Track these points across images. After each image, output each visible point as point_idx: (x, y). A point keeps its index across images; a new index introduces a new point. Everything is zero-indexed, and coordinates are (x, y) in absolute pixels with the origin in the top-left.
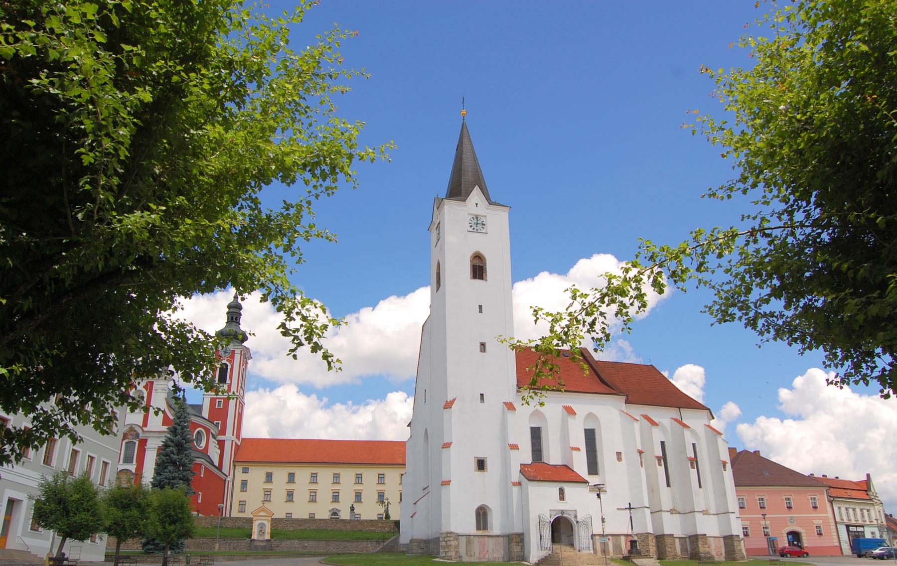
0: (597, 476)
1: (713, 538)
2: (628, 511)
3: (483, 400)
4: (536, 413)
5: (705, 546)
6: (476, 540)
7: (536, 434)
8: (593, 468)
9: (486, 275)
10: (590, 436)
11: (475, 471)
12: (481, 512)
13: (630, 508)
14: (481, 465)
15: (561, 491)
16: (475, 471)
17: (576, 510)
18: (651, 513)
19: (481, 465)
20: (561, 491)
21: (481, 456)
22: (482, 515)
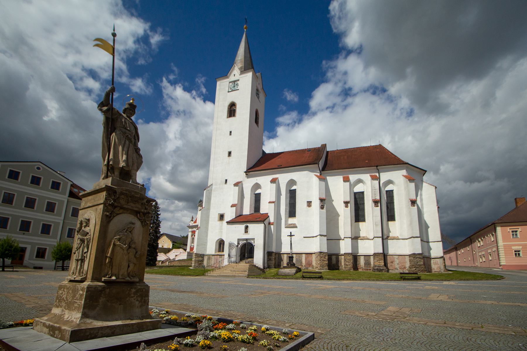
0: (295, 218)
1: (398, 256)
2: (289, 238)
5: (380, 261)
6: (213, 257)
7: (257, 198)
8: (292, 213)
10: (292, 195)
11: (218, 221)
12: (222, 243)
15: (247, 227)
16: (218, 221)
18: (327, 240)
20: (247, 227)
21: (221, 212)
22: (221, 244)
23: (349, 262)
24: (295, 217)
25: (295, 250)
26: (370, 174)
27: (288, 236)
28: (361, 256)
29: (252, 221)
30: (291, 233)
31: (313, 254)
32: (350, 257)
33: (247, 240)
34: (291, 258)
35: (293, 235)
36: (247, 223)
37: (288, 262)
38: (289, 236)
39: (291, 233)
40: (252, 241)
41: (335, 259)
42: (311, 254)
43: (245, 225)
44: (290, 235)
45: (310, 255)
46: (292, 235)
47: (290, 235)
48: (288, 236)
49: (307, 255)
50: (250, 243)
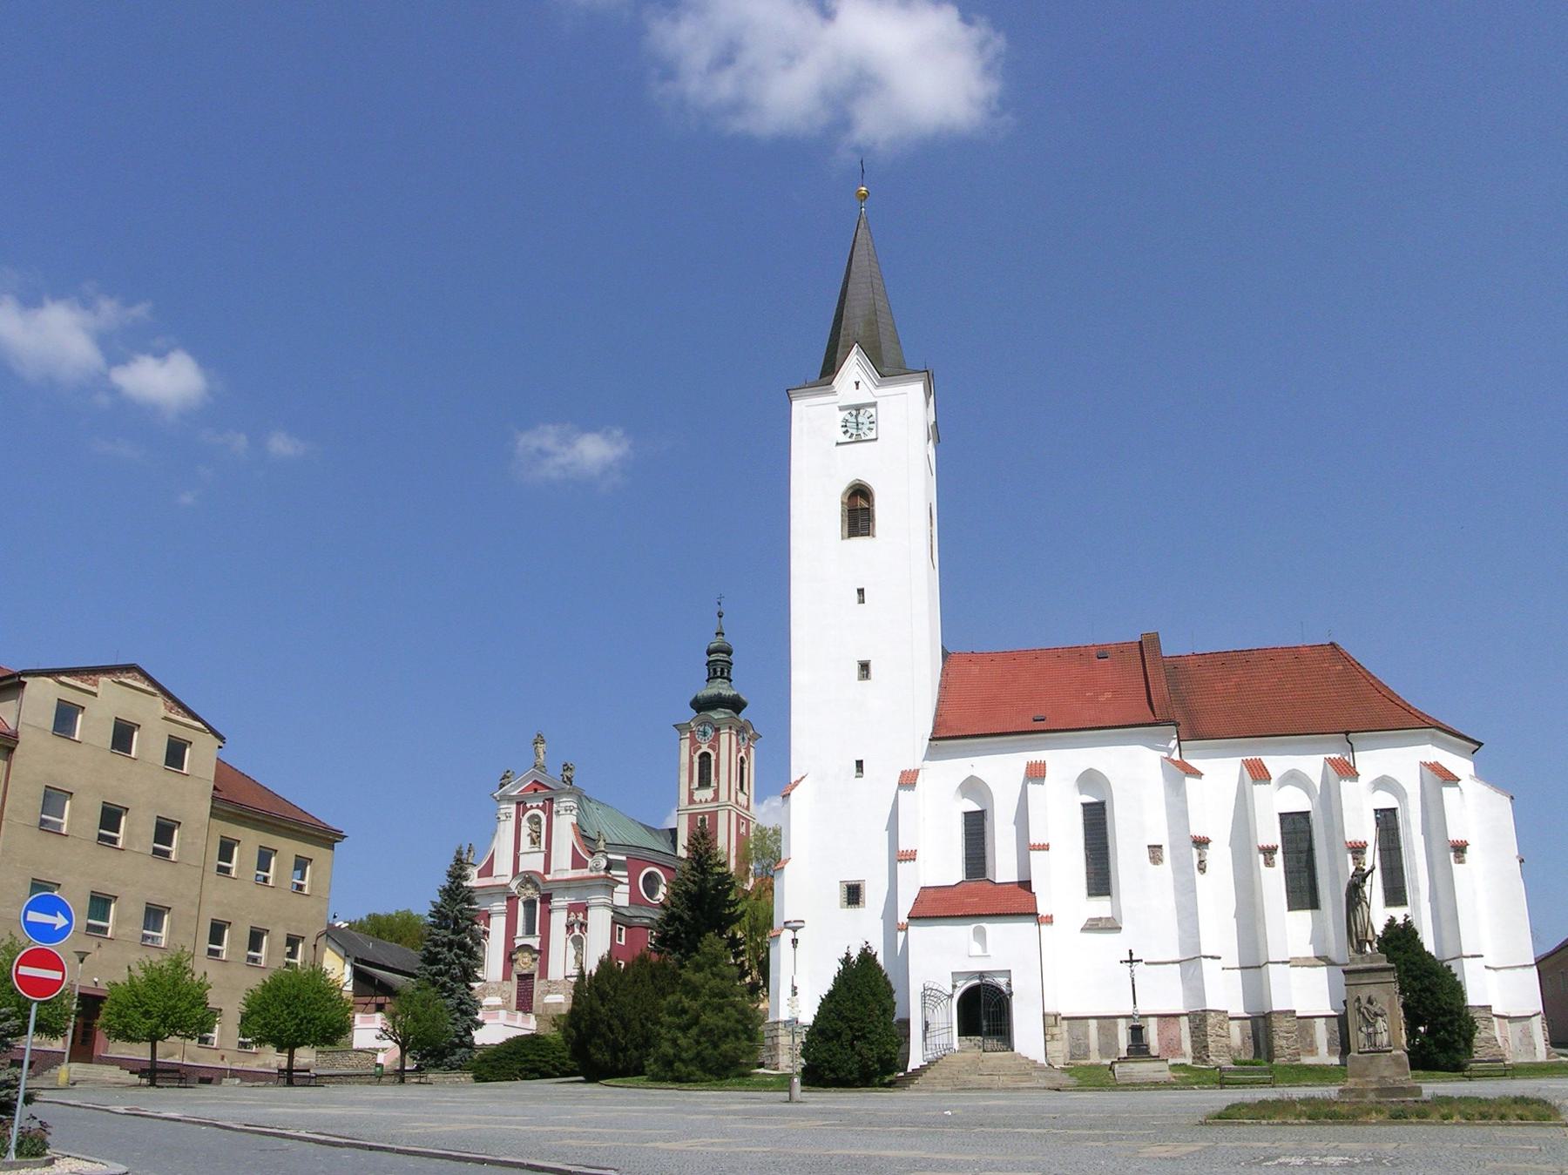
3: (862, 771)
4: (972, 786)
9: (874, 525)
13: (1131, 961)
14: (853, 894)
17: (1010, 971)
19: (853, 894)
23: (1287, 1039)
24: (1090, 895)
25: (1143, 1008)
26: (1244, 758)
27: (1121, 962)
28: (1316, 1020)
29: (1007, 915)
30: (1131, 954)
31: (1181, 1018)
32: (1288, 1022)
33: (981, 975)
34: (1137, 1032)
35: (1137, 961)
36: (981, 919)
37: (1130, 1043)
38: (1126, 962)
39: (1131, 954)
40: (1001, 982)
41: (1238, 1029)
42: (1176, 1016)
43: (974, 926)
44: (1128, 959)
45: (1172, 1020)
46: (1134, 958)
47: (1128, 959)
48: (1121, 962)
49: (1164, 1019)
50: (993, 986)
